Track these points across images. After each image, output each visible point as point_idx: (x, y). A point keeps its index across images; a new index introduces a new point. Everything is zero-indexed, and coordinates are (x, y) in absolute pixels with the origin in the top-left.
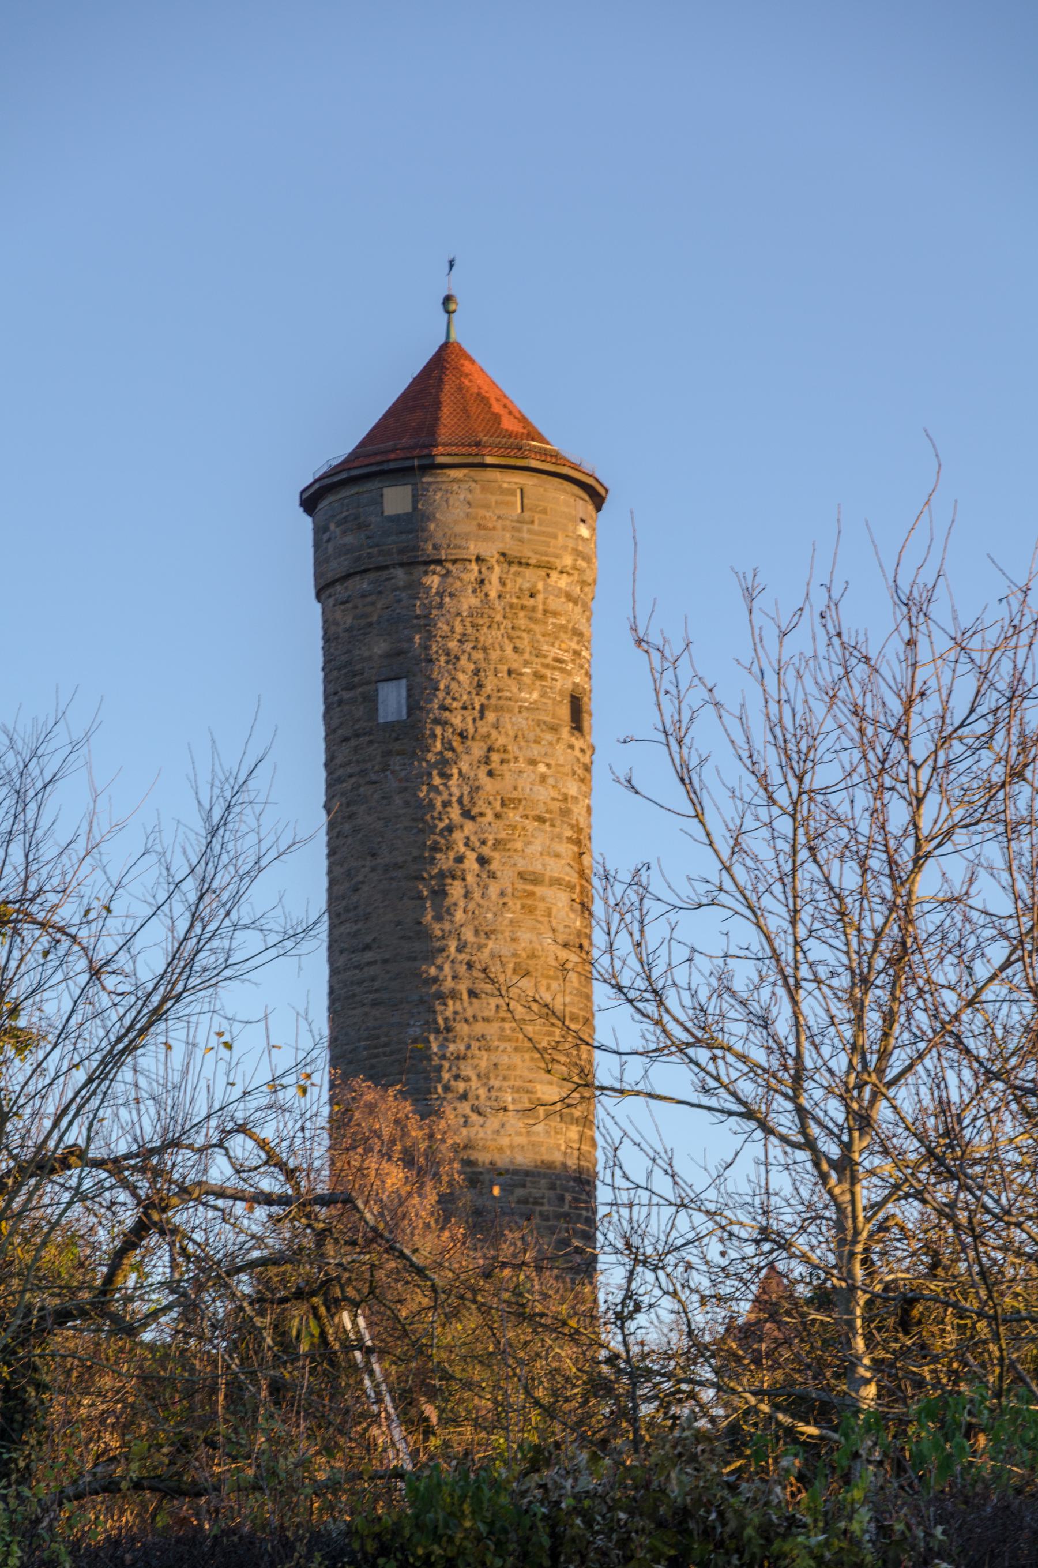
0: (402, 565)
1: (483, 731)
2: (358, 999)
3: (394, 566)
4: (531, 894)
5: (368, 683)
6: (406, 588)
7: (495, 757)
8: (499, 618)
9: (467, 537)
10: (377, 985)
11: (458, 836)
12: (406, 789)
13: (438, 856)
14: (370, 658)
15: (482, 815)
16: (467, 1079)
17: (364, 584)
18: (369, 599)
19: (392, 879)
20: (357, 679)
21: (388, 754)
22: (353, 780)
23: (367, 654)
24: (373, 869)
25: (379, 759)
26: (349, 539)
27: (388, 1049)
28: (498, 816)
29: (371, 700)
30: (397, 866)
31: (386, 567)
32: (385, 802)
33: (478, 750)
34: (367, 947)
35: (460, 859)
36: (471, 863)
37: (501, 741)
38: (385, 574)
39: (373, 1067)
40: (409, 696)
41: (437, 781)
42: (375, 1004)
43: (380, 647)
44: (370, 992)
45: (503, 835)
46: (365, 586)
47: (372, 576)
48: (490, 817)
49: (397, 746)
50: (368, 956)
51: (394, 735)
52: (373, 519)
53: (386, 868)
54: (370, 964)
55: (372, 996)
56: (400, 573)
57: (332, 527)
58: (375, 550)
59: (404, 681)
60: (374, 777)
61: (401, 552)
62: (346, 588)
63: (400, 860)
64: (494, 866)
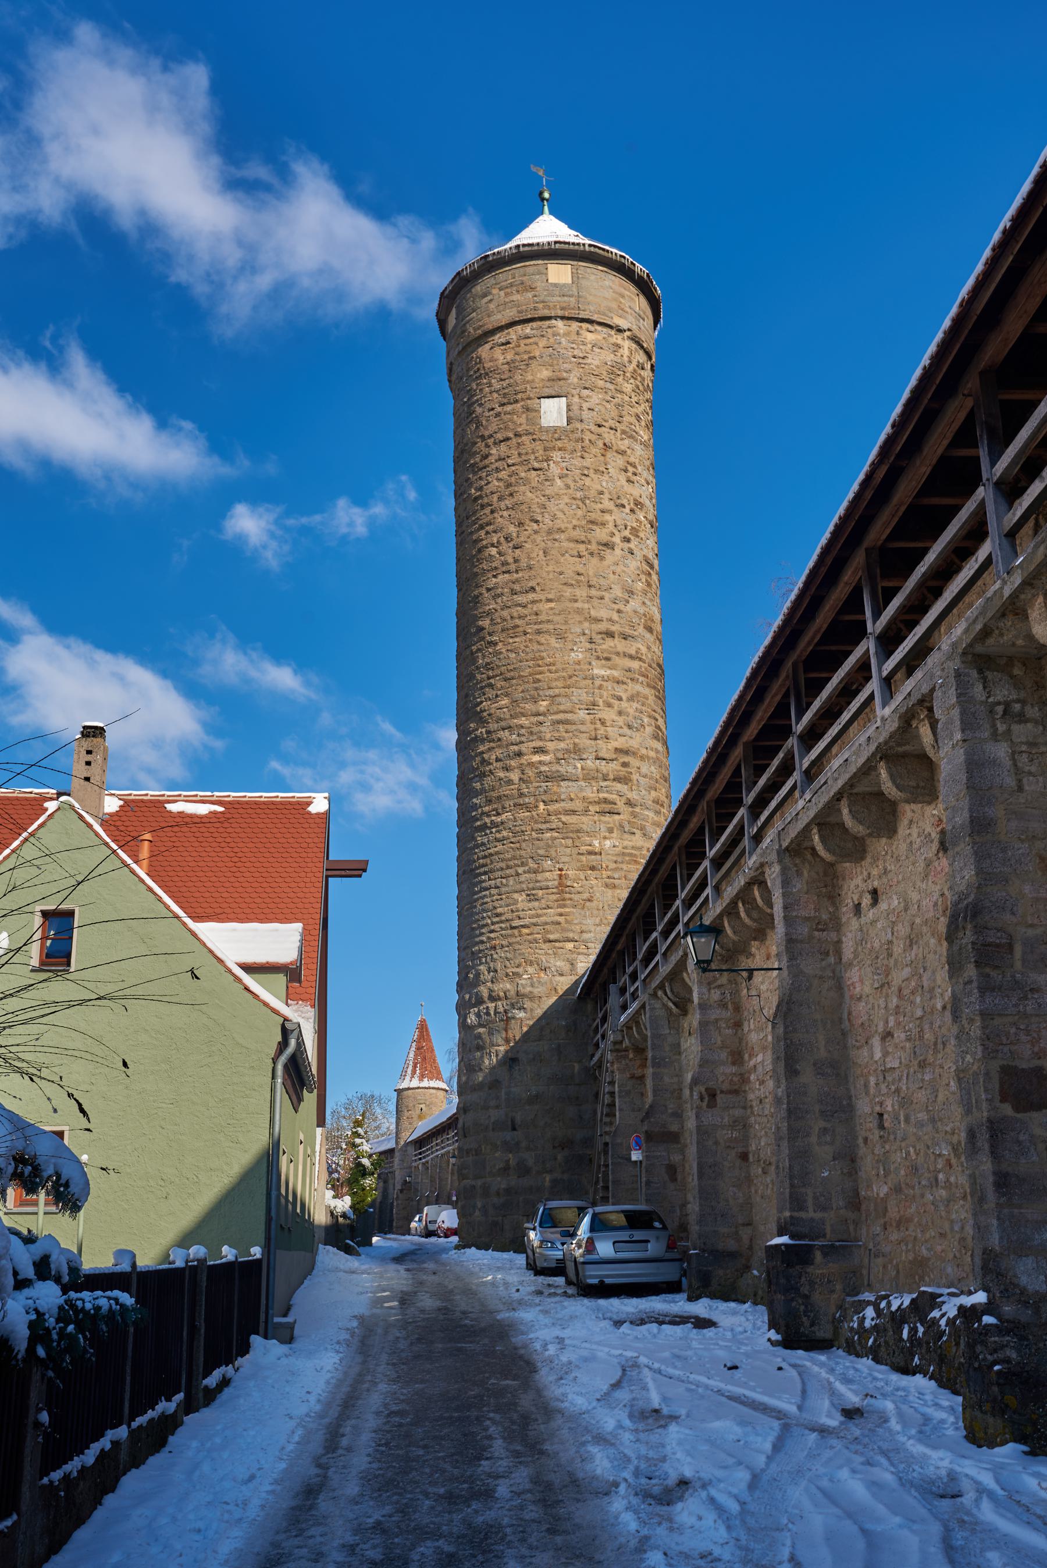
0: (563, 318)
1: (623, 448)
2: (521, 629)
3: (556, 318)
4: (650, 574)
5: (529, 398)
6: (567, 334)
7: (630, 468)
8: (628, 375)
9: (610, 310)
10: (543, 617)
11: (607, 517)
12: (567, 475)
13: (594, 527)
14: (533, 381)
15: (623, 506)
16: (620, 699)
17: (527, 329)
18: (531, 340)
19: (555, 540)
20: (519, 396)
21: (554, 448)
22: (513, 468)
23: (530, 378)
24: (536, 532)
25: (541, 452)
26: (516, 297)
27: (554, 668)
28: (632, 511)
29: (532, 412)
30: (561, 531)
31: (549, 318)
32: (548, 483)
33: (620, 461)
34: (533, 589)
35: (613, 534)
36: (617, 539)
37: (632, 460)
38: (547, 323)
39: (539, 681)
40: (569, 410)
41: (591, 473)
42: (539, 632)
43: (546, 373)
44: (535, 623)
45: (635, 525)
46: (528, 331)
47: (535, 324)
48: (627, 510)
49: (559, 444)
50: (531, 596)
51: (556, 436)
52: (539, 284)
53: (549, 532)
54: (534, 602)
55: (536, 627)
56: (560, 323)
57: (495, 291)
58: (541, 306)
59: (564, 399)
60: (536, 465)
61: (562, 309)
62: (508, 334)
63: (563, 526)
64: (632, 545)
